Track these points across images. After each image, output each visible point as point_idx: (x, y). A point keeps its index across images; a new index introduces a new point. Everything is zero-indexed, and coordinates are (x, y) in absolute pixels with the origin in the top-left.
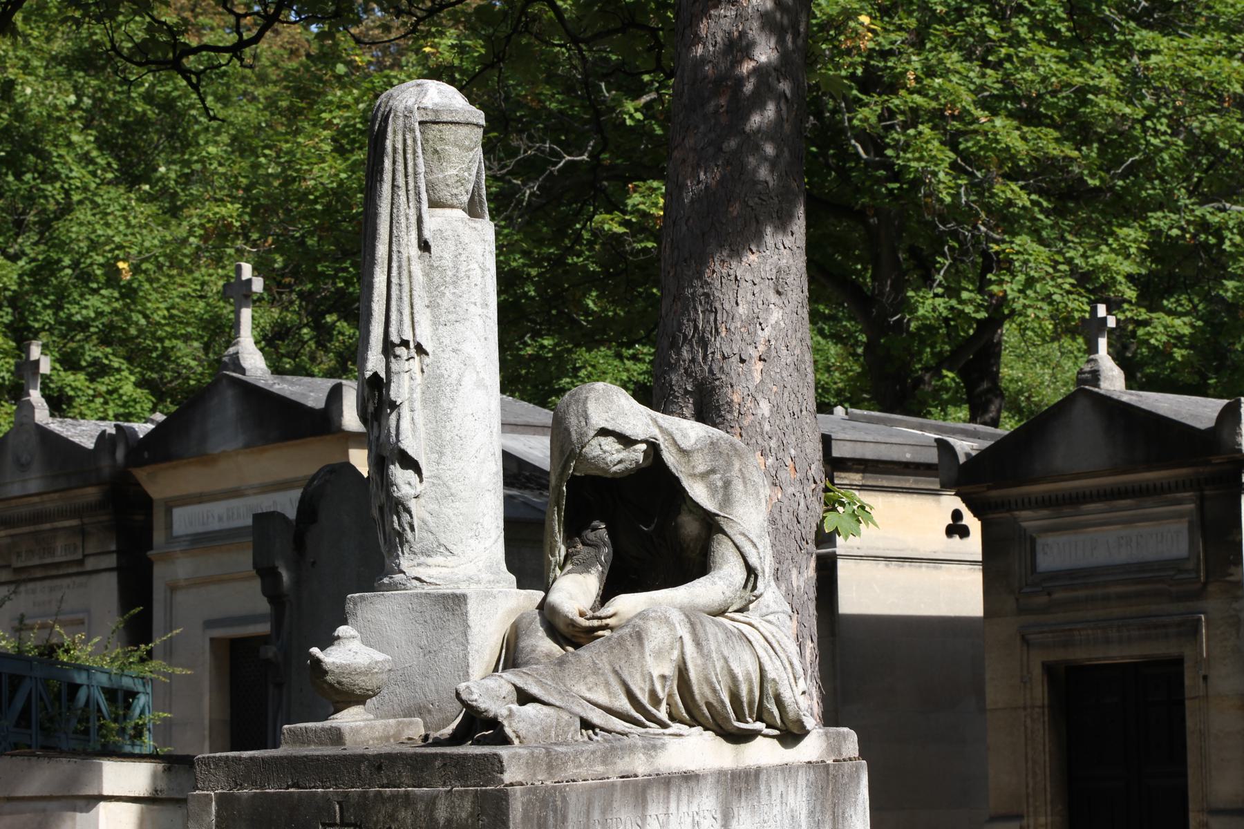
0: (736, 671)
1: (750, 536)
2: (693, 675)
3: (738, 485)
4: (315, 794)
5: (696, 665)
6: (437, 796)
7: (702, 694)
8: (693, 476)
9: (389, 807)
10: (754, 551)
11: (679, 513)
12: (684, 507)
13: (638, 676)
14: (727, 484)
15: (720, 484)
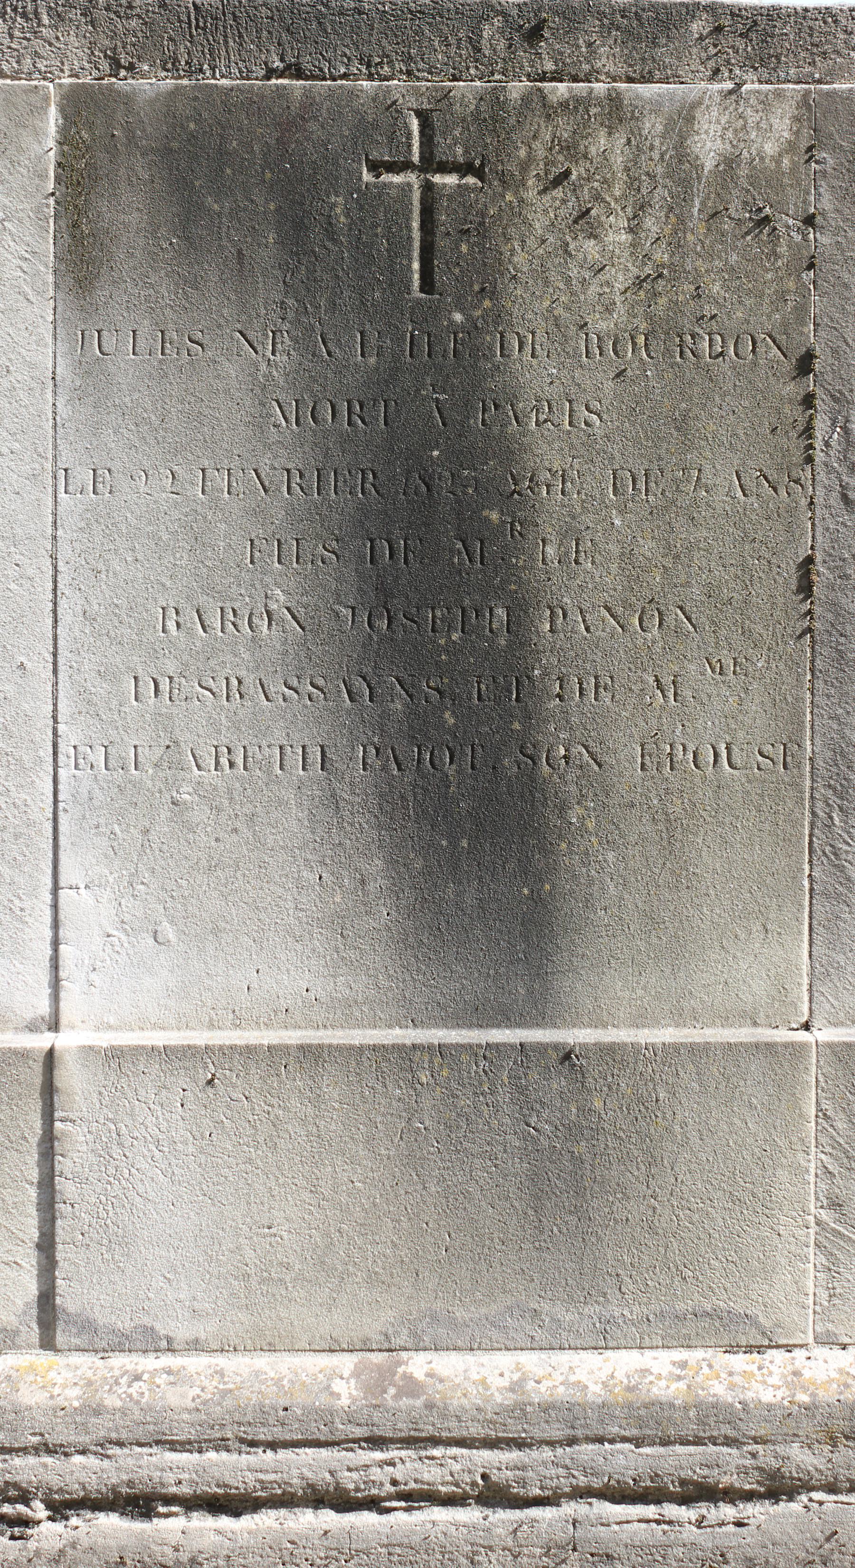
4: (352, 94)
6: (697, 104)
9: (565, 127)
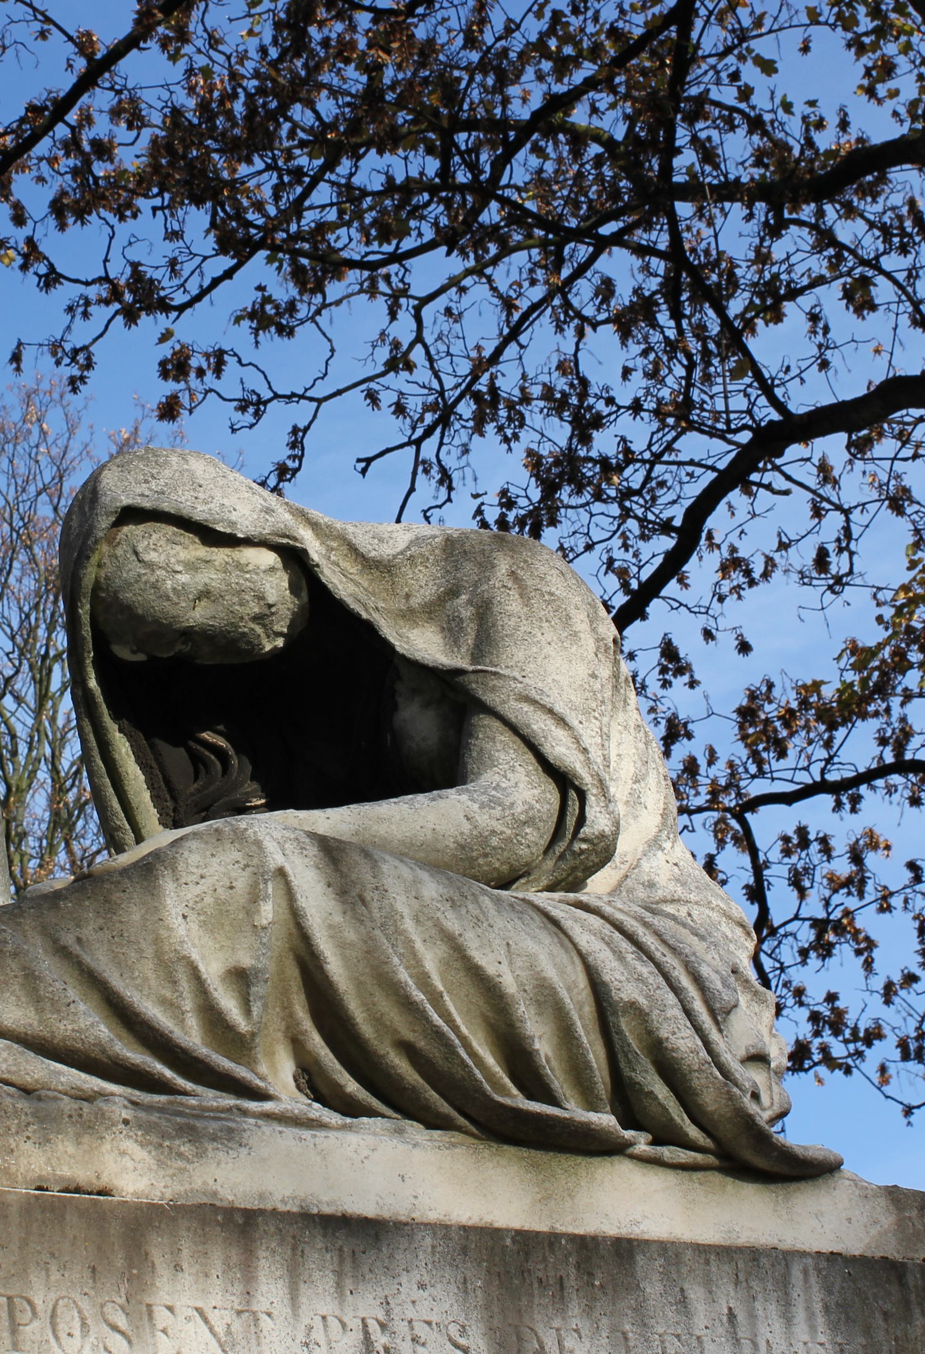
0: (491, 970)
1: (546, 701)
2: (336, 967)
3: (510, 605)
5: (342, 946)
7: (378, 1020)
8: (409, 616)
10: (560, 733)
11: (395, 708)
12: (400, 687)
13: (148, 968)
14: (484, 611)
15: (467, 613)
